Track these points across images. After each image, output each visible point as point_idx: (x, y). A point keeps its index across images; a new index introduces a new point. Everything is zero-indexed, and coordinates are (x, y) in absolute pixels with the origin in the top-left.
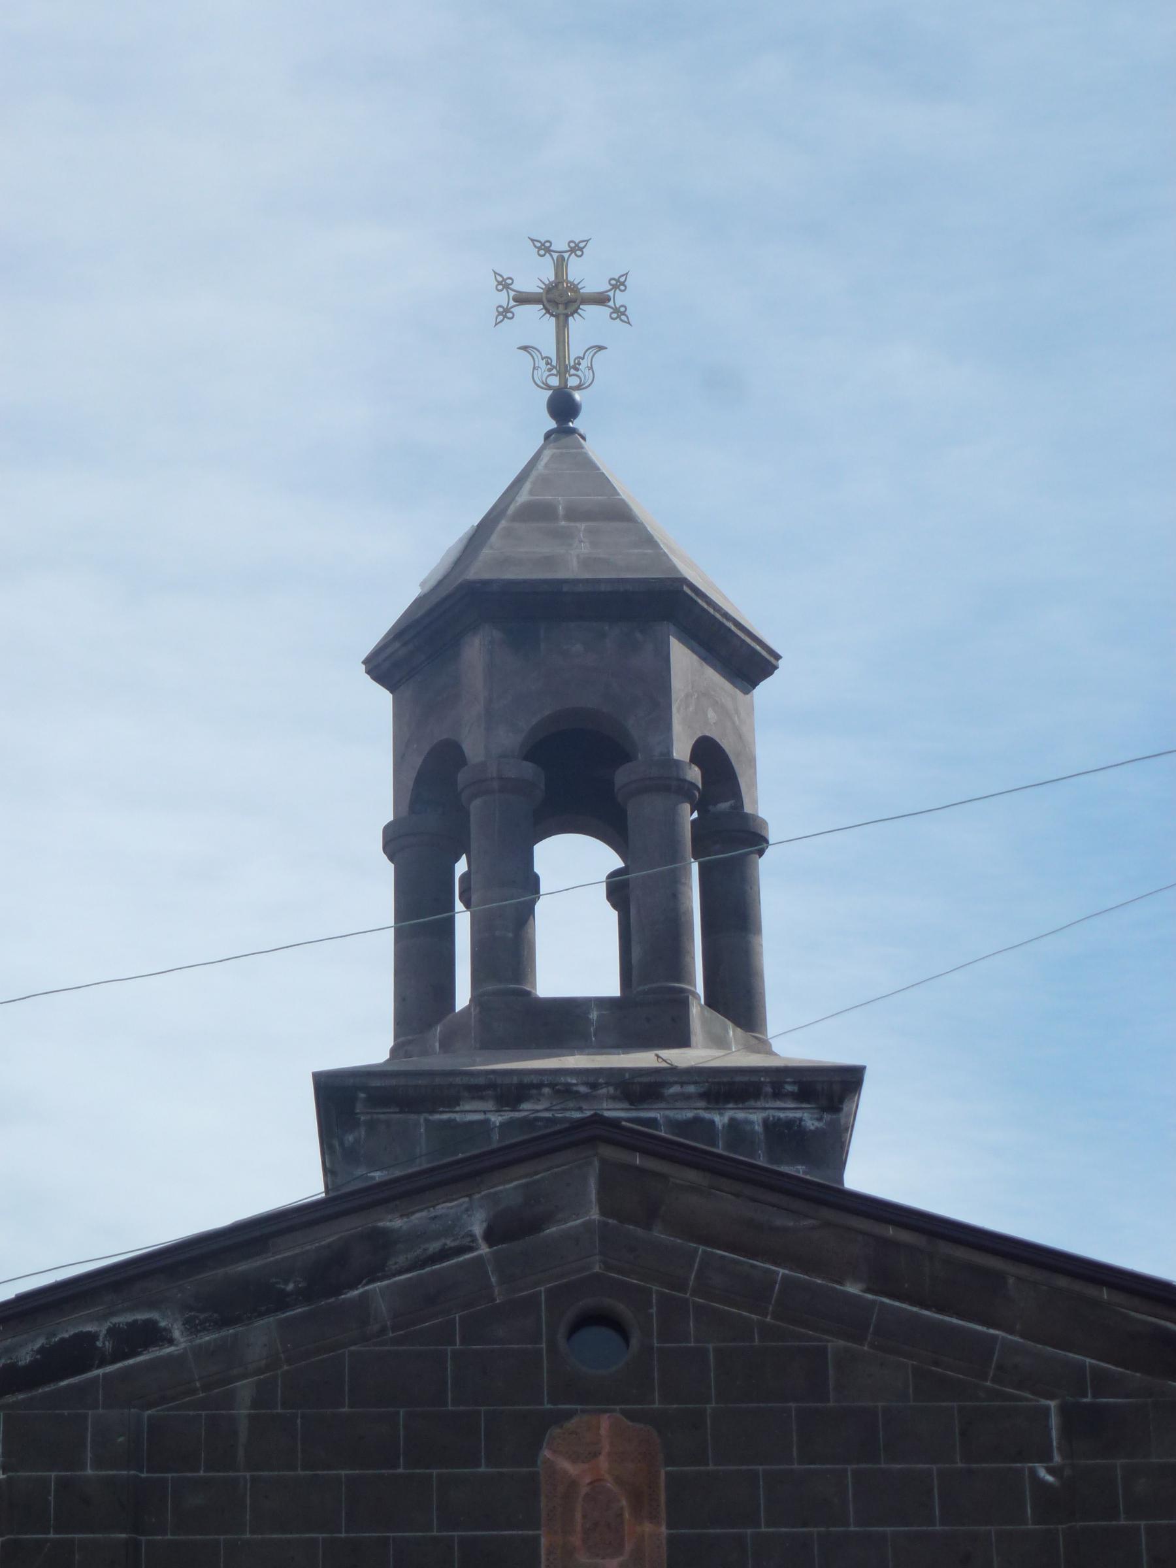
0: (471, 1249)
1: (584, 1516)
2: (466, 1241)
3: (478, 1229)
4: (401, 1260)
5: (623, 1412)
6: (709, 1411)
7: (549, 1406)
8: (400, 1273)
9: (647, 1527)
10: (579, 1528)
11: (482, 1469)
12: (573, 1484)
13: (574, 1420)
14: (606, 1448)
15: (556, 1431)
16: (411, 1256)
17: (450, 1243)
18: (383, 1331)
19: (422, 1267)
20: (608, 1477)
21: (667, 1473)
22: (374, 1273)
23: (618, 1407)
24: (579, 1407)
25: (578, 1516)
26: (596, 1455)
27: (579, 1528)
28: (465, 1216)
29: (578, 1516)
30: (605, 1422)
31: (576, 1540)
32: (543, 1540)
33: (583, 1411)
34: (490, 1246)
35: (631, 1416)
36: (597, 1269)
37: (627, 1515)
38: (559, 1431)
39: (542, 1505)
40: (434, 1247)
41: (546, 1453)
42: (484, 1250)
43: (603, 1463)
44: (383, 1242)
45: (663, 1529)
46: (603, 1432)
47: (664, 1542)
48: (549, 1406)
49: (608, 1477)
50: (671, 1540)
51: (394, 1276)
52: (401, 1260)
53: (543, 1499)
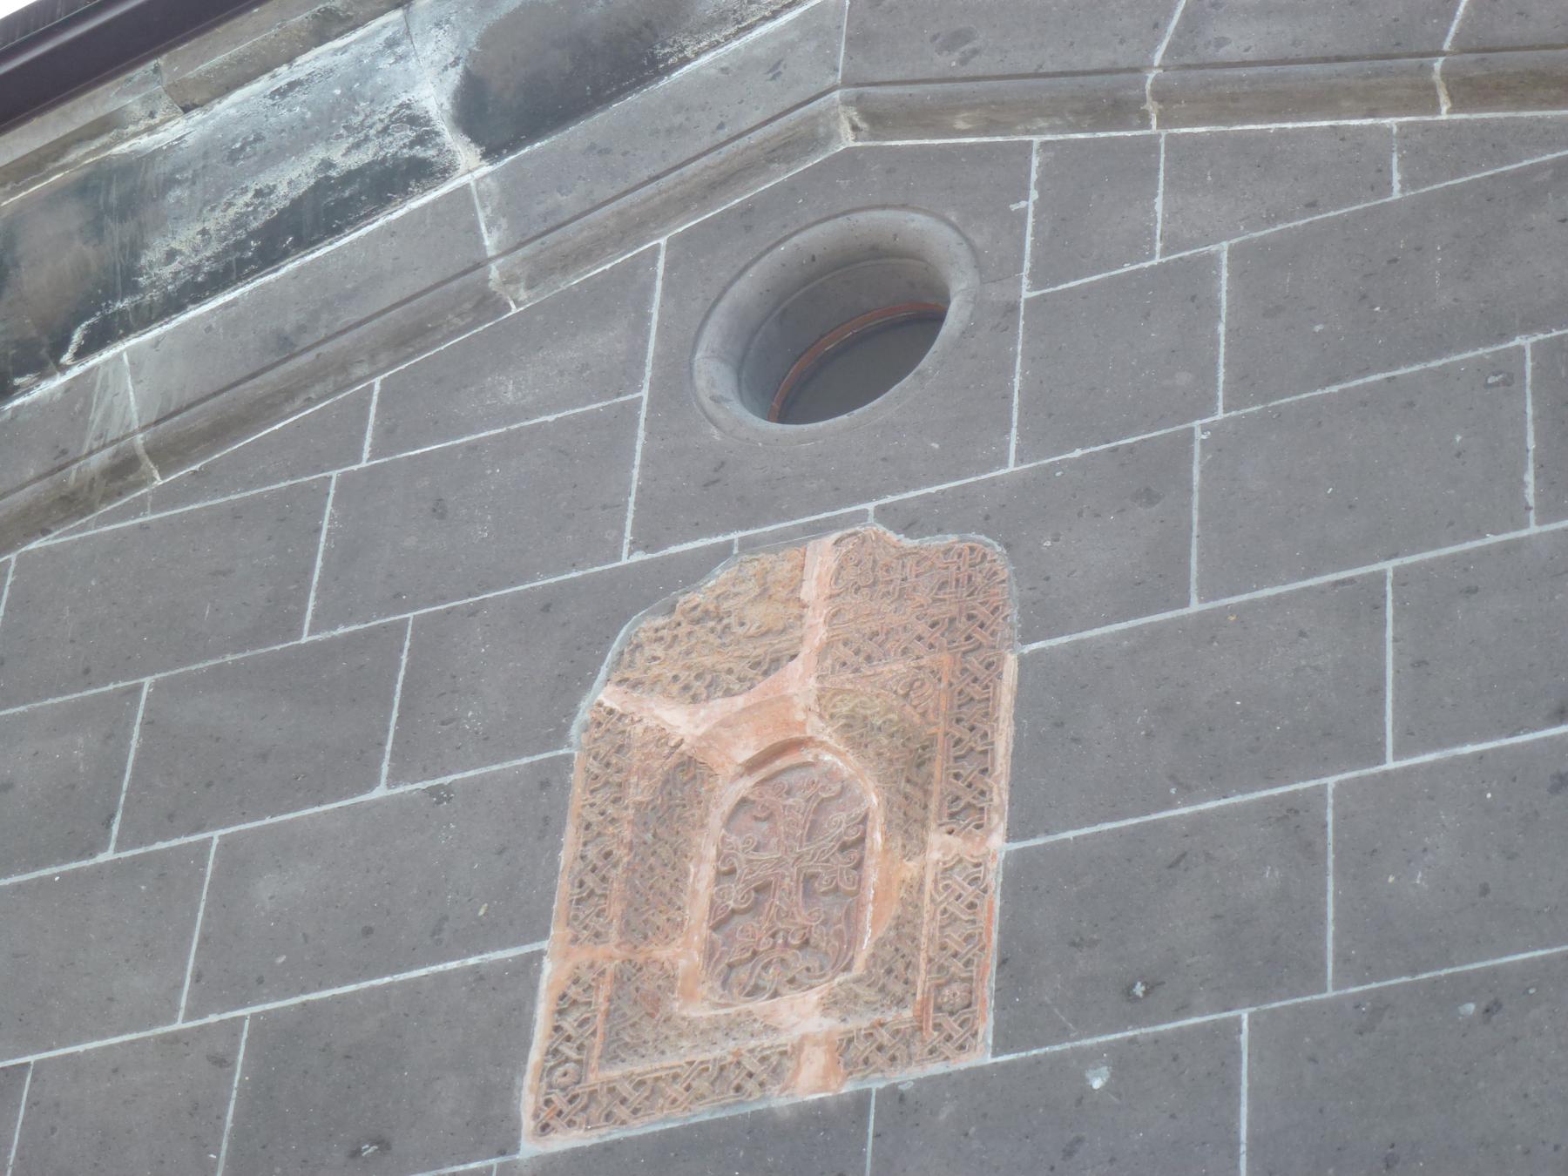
0: (421, 172)
1: (726, 874)
2: (398, 144)
3: (433, 95)
4: (178, 245)
5: (883, 513)
6: (1200, 436)
7: (639, 556)
8: (194, 292)
9: (940, 845)
10: (697, 912)
11: (380, 792)
12: (688, 771)
13: (721, 576)
14: (816, 631)
15: (645, 624)
16: (217, 220)
17: (345, 158)
18: (123, 471)
19: (269, 257)
20: (816, 727)
21: (1023, 661)
22: (104, 308)
23: (870, 506)
24: (735, 536)
25: (701, 876)
26: (773, 664)
27: (697, 912)
28: (385, 63)
29: (701, 876)
30: (822, 557)
31: (683, 954)
32: (548, 966)
33: (747, 545)
34: (491, 153)
35: (907, 521)
36: (847, 140)
37: (877, 838)
38: (660, 621)
39: (565, 857)
40: (291, 178)
41: (605, 695)
42: (470, 167)
43: (799, 681)
44: (122, 197)
45: (998, 843)
46: (809, 591)
47: (994, 879)
48: (639, 556)
49: (824, 732)
50: (1019, 873)
51: (174, 304)
52: (178, 245)
53: (571, 837)
